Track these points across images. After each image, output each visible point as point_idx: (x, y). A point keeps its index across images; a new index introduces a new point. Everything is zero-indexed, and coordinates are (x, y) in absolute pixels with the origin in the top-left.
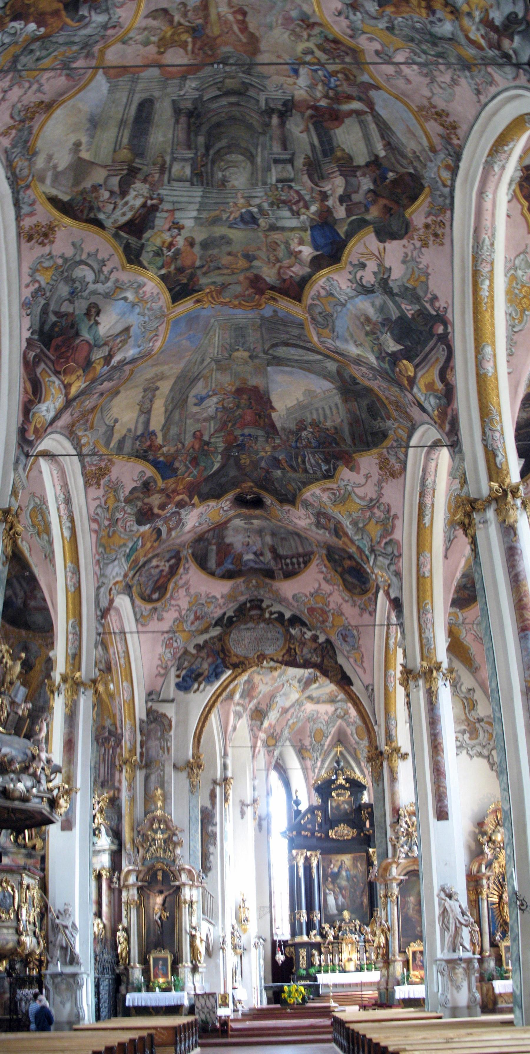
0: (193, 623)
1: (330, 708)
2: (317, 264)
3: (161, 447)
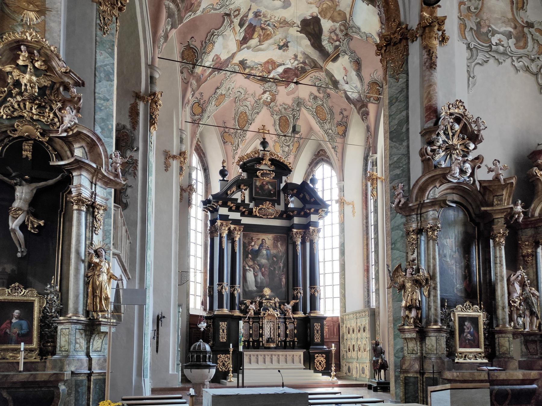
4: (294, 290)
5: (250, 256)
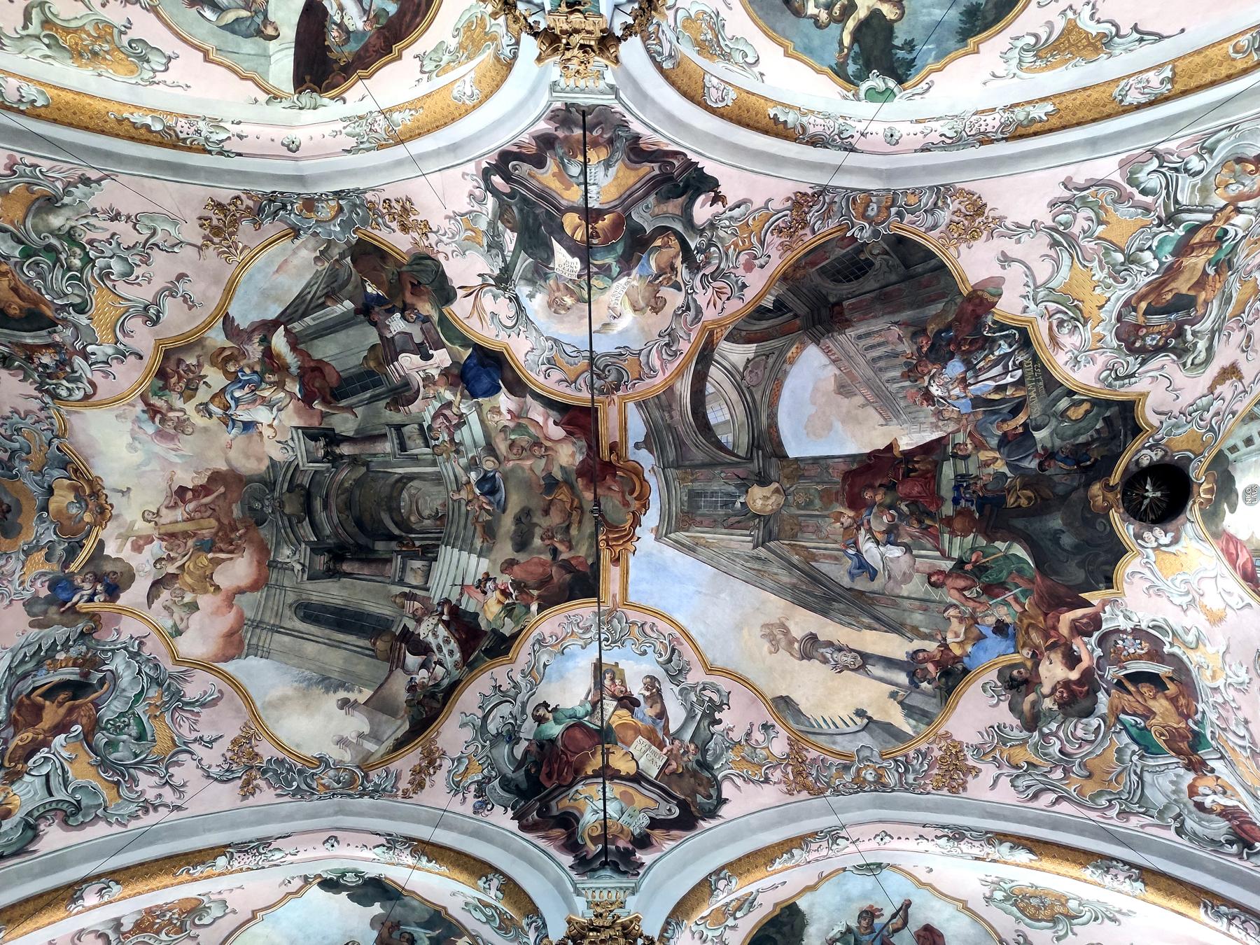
2: (518, 387)
3: (945, 646)
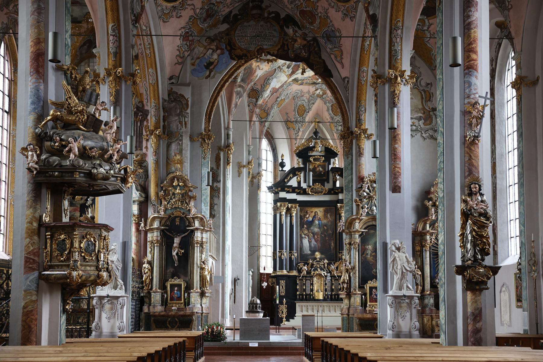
0: (205, 20)
1: (312, 89)
4: (339, 253)
5: (305, 226)
